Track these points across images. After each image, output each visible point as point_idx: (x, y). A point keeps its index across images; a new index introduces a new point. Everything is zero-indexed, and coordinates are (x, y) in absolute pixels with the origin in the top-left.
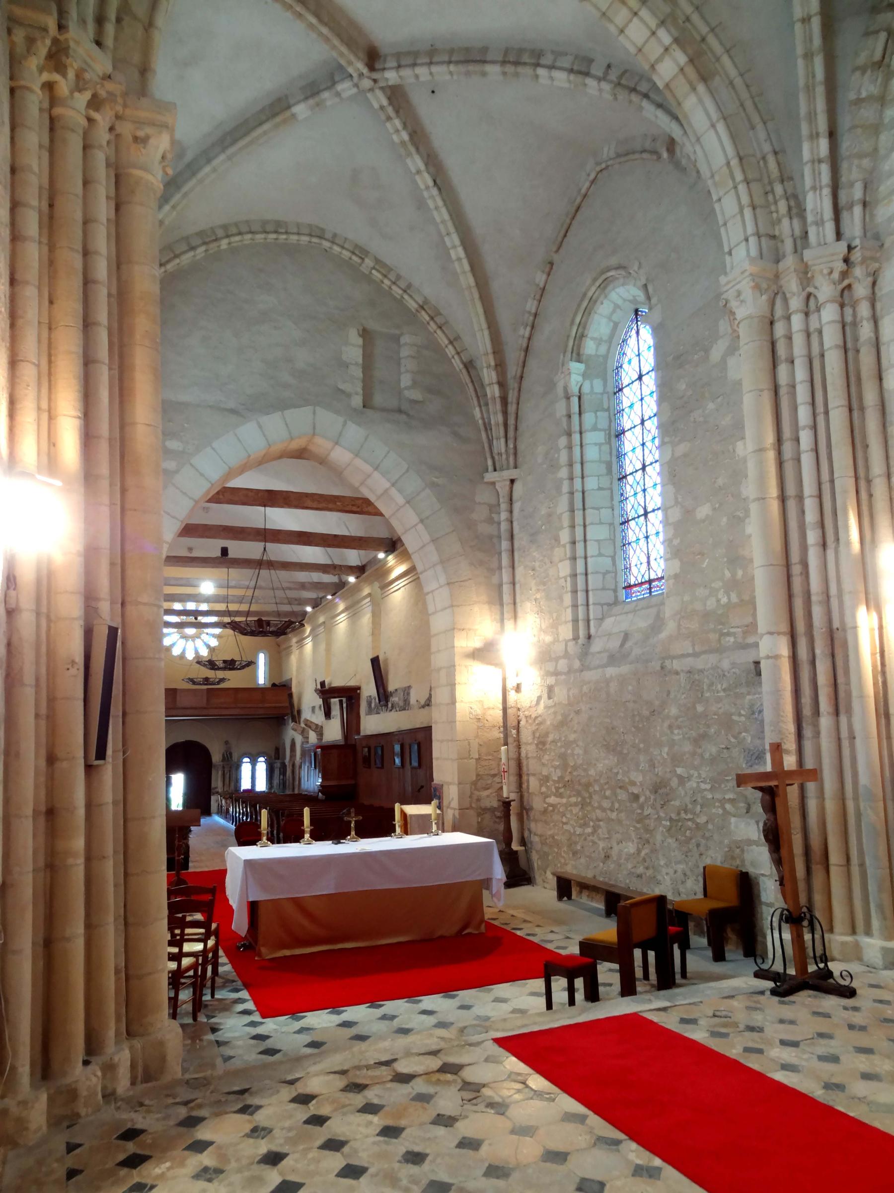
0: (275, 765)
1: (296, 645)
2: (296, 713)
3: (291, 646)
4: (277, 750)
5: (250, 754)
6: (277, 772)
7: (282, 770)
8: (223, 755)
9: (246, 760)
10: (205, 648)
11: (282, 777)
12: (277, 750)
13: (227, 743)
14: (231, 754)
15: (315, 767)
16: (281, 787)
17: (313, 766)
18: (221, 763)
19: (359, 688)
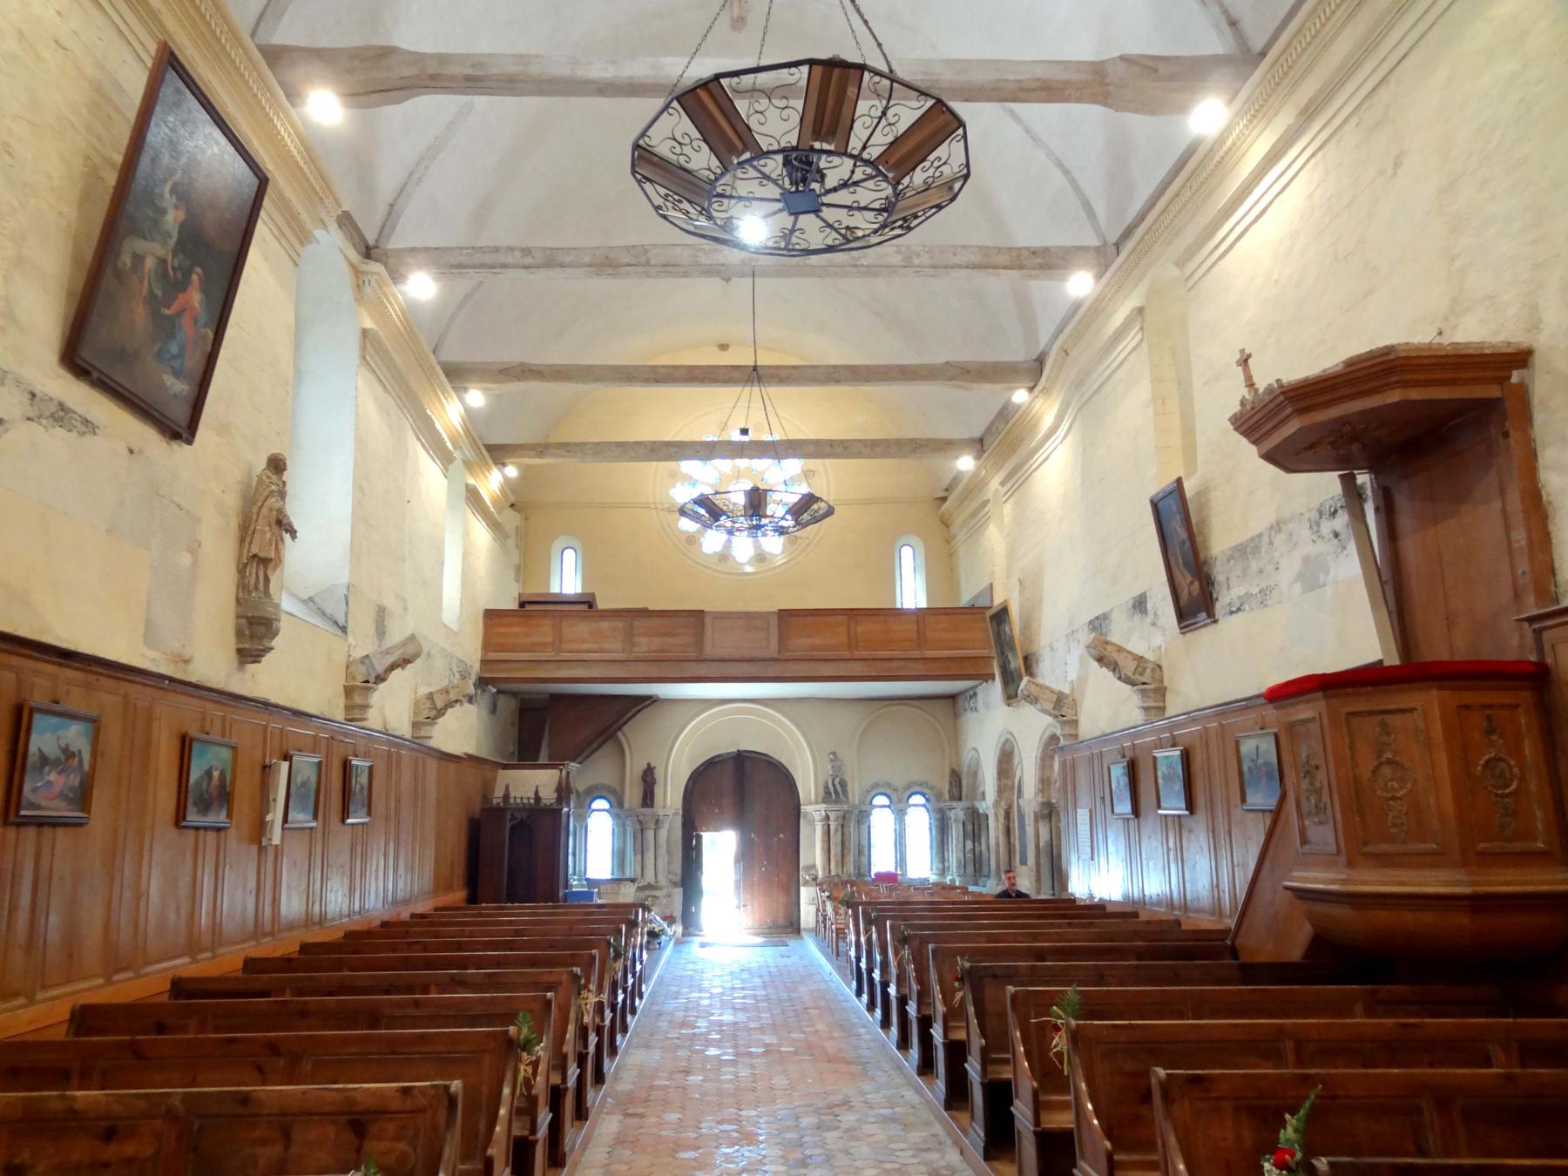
0: (952, 814)
1: (1003, 490)
2: (1016, 663)
4: (956, 776)
5: (890, 785)
6: (955, 832)
7: (970, 827)
8: (826, 787)
9: (881, 800)
11: (969, 845)
12: (956, 776)
14: (843, 784)
15: (1136, 811)
16: (970, 869)
17: (1124, 807)
19: (1522, 358)
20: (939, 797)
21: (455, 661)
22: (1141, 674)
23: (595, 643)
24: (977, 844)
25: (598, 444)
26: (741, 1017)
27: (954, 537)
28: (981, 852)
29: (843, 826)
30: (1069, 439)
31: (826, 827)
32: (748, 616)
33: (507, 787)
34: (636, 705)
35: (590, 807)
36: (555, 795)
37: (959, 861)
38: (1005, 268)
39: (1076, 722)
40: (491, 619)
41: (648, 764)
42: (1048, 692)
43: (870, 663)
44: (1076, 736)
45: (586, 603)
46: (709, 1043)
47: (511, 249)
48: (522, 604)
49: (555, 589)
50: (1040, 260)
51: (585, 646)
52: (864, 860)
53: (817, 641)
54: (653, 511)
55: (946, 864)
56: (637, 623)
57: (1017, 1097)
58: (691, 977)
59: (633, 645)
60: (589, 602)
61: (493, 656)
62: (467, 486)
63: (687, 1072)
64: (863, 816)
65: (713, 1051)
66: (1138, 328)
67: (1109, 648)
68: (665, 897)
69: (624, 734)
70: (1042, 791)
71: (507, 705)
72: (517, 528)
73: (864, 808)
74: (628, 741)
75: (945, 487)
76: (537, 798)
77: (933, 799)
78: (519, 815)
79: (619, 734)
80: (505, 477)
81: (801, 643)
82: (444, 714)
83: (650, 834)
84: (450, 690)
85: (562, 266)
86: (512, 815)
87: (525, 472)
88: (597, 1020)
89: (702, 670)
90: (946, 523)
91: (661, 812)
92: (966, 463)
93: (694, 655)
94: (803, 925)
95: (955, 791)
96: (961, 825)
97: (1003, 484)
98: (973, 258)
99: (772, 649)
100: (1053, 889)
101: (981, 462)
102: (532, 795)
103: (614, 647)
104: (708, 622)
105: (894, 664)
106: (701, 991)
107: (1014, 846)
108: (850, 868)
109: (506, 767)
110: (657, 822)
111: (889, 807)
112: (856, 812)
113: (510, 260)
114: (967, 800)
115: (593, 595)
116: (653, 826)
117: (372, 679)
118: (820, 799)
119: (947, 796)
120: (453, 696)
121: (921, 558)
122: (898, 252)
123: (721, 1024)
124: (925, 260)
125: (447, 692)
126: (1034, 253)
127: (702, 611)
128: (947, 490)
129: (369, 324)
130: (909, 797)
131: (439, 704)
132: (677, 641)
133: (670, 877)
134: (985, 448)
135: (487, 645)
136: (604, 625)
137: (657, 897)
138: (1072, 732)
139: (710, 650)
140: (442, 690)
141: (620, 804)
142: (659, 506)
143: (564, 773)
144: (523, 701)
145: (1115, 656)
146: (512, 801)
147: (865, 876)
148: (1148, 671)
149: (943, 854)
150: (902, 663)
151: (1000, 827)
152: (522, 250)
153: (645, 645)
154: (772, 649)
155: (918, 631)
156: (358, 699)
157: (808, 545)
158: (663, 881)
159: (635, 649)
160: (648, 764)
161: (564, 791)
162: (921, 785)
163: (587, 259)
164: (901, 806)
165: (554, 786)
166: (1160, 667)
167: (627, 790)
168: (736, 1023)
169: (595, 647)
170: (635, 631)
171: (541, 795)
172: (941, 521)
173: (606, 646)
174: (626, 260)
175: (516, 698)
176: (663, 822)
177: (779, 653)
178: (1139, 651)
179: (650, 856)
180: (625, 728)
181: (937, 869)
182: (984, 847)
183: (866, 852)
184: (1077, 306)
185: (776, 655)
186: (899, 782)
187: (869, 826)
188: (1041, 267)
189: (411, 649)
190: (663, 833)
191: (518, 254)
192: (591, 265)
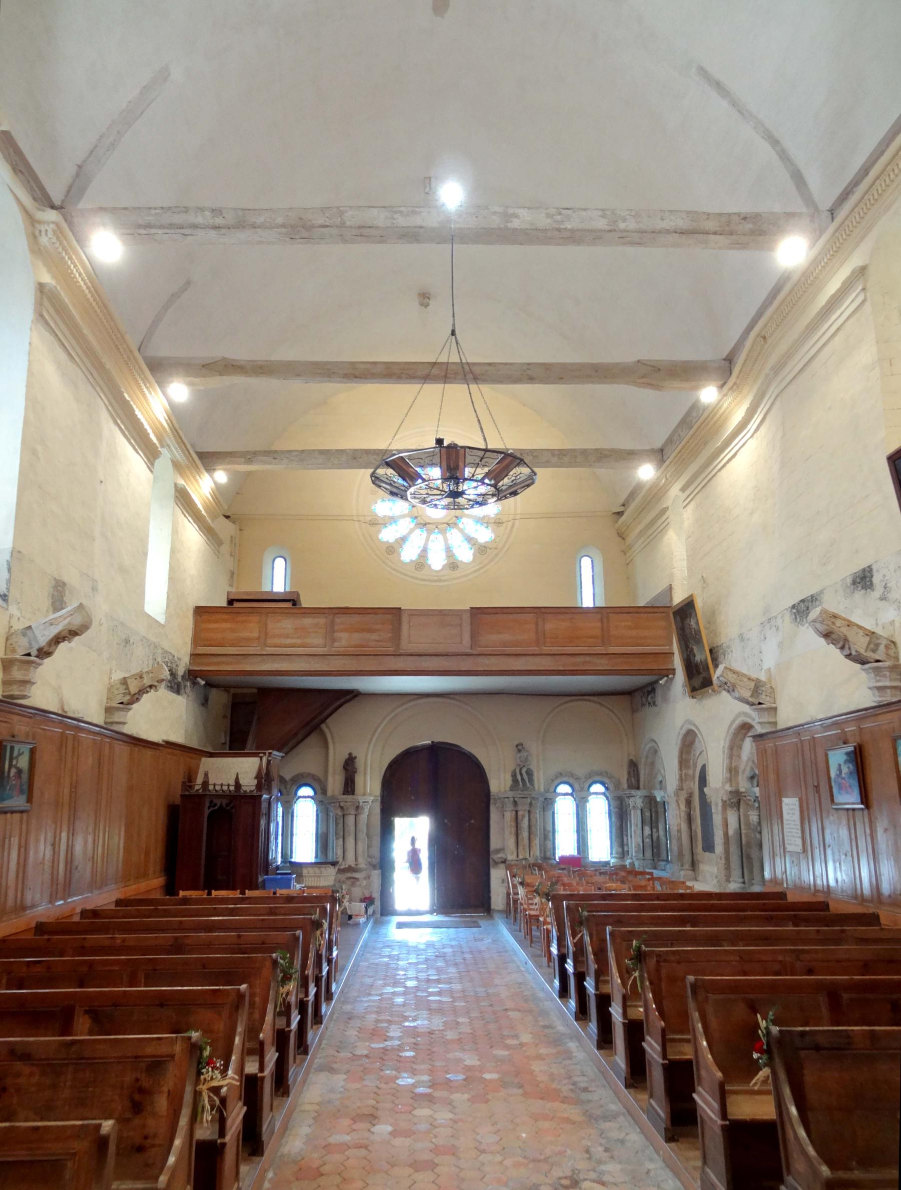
0: (631, 802)
1: (683, 496)
3: (665, 510)
4: (633, 766)
5: (572, 775)
6: (635, 818)
7: (647, 814)
8: (514, 775)
9: (564, 788)
10: (466, 546)
12: (633, 766)
13: (519, 748)
14: (530, 773)
16: (648, 854)
17: (850, 798)
18: (510, 794)
20: (617, 786)
21: (160, 651)
22: (874, 651)
23: (298, 638)
24: (654, 830)
25: (303, 451)
26: (437, 1023)
27: (630, 547)
28: (658, 837)
29: (529, 812)
30: (763, 429)
31: (514, 813)
32: (442, 613)
33: (206, 775)
34: (338, 699)
35: (296, 793)
36: (255, 782)
37: (638, 846)
38: (715, 233)
39: (775, 709)
40: (201, 617)
41: (350, 754)
42: (745, 679)
43: (558, 657)
44: (775, 723)
45: (291, 601)
46: (402, 1065)
47: (201, 209)
48: (231, 602)
49: (266, 588)
50: (750, 226)
51: (288, 641)
52: (550, 845)
53: (506, 637)
54: (357, 523)
55: (626, 849)
56: (338, 620)
57: (789, 1172)
58: (387, 964)
59: (334, 640)
60: (294, 600)
61: (202, 650)
62: (176, 485)
63: (372, 1118)
64: (548, 803)
65: (406, 1080)
66: (860, 287)
67: (838, 623)
68: (365, 878)
69: (328, 727)
70: (730, 780)
71: (219, 698)
72: (232, 537)
73: (549, 796)
74: (331, 733)
75: (622, 502)
76: (238, 785)
77: (611, 787)
78: (218, 802)
79: (323, 726)
80: (215, 483)
81: (492, 639)
82: (138, 700)
83: (350, 820)
84: (144, 676)
85: (254, 226)
86: (211, 802)
87: (234, 476)
88: (301, 996)
89: (399, 664)
90: (622, 536)
91: (361, 799)
92: (646, 472)
93: (391, 650)
94: (493, 906)
95: (633, 779)
96: (639, 812)
97: (683, 490)
98: (681, 223)
99: (465, 644)
100: (743, 877)
101: (661, 470)
102: (232, 782)
103: (316, 642)
104: (405, 618)
105: (580, 659)
106: (396, 983)
107: (696, 832)
108: (536, 851)
109: (211, 755)
110: (358, 807)
111: (571, 795)
112: (542, 799)
113: (199, 220)
114: (644, 789)
115: (298, 594)
116: (353, 812)
117: (34, 652)
118: (508, 788)
119: (625, 786)
120: (147, 681)
121: (599, 568)
122: (603, 216)
123: (413, 1032)
124: (631, 225)
125: (141, 677)
126: (745, 218)
127: (400, 608)
128: (624, 505)
129: (47, 278)
130: (590, 786)
131: (133, 689)
132: (374, 636)
133: (369, 860)
134: (665, 458)
135: (197, 640)
136: (308, 621)
137: (357, 879)
138: (772, 720)
139: (406, 645)
140: (137, 674)
141: (324, 792)
142: (361, 518)
143: (265, 760)
144: (235, 695)
145: (844, 630)
146: (211, 788)
147: (549, 859)
148: (882, 647)
149: (623, 841)
150: (588, 658)
151: (683, 814)
152: (213, 210)
153: (345, 640)
154: (465, 644)
155: (602, 629)
156: (17, 674)
157: (496, 555)
158: (362, 864)
159: (336, 644)
160: (350, 754)
161: (264, 779)
162: (601, 774)
163: (280, 220)
164: (583, 794)
165: (254, 774)
166: (894, 643)
167: (330, 779)
168: (431, 1033)
169: (299, 641)
170: (336, 627)
171: (241, 782)
172: (618, 533)
173: (308, 641)
174: (321, 221)
175: (228, 692)
176: (363, 809)
177: (471, 648)
178: (869, 625)
179: (350, 841)
180: (328, 721)
181: (617, 853)
182: (661, 833)
183: (551, 837)
184: (785, 278)
185: (468, 651)
186: (581, 772)
187: (554, 813)
188: (752, 233)
189: (77, 621)
190: (364, 817)
191: (207, 213)
192: (283, 226)
